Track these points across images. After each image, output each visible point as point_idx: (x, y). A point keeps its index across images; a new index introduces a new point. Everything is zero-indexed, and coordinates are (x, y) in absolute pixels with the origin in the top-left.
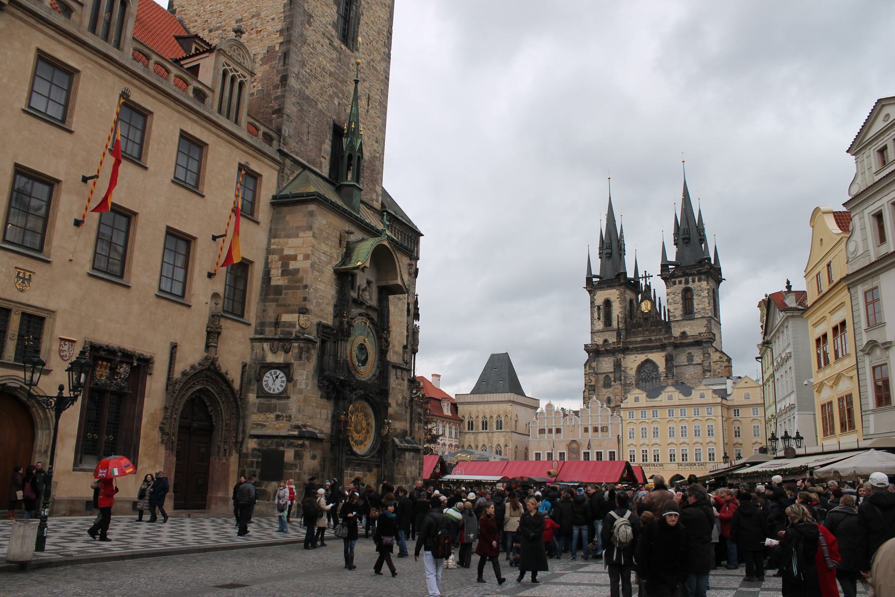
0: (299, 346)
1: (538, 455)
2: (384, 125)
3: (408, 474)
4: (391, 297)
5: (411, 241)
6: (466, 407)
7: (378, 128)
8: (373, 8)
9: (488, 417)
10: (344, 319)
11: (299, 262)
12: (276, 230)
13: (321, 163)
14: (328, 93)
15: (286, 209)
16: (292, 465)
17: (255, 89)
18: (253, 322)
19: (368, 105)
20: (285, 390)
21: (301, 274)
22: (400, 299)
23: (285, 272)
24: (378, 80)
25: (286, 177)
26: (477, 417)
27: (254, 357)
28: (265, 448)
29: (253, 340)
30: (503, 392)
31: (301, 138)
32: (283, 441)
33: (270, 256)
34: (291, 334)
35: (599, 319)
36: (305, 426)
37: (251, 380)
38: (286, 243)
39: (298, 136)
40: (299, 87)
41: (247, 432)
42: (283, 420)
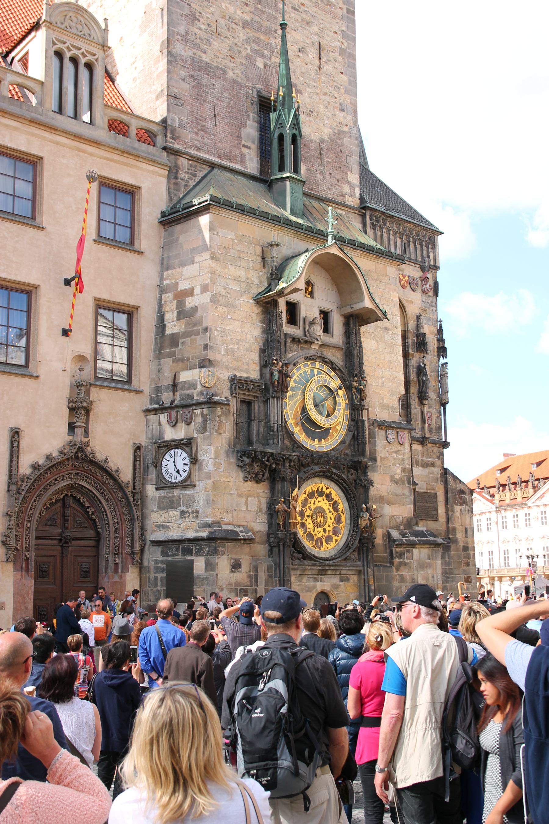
0: (202, 413)
2: (353, 83)
5: (421, 246)
7: (342, 90)
10: (274, 368)
11: (197, 297)
12: (169, 258)
13: (243, 155)
14: (244, 53)
16: (203, 579)
18: (147, 388)
19: (320, 59)
22: (386, 329)
23: (182, 314)
24: (334, 18)
25: (182, 183)
27: (150, 436)
28: (170, 558)
29: (148, 411)
31: (203, 126)
33: (163, 296)
34: (191, 397)
36: (218, 524)
37: (148, 467)
38: (181, 274)
39: (198, 123)
40: (190, 53)
41: (148, 537)
42: (189, 517)
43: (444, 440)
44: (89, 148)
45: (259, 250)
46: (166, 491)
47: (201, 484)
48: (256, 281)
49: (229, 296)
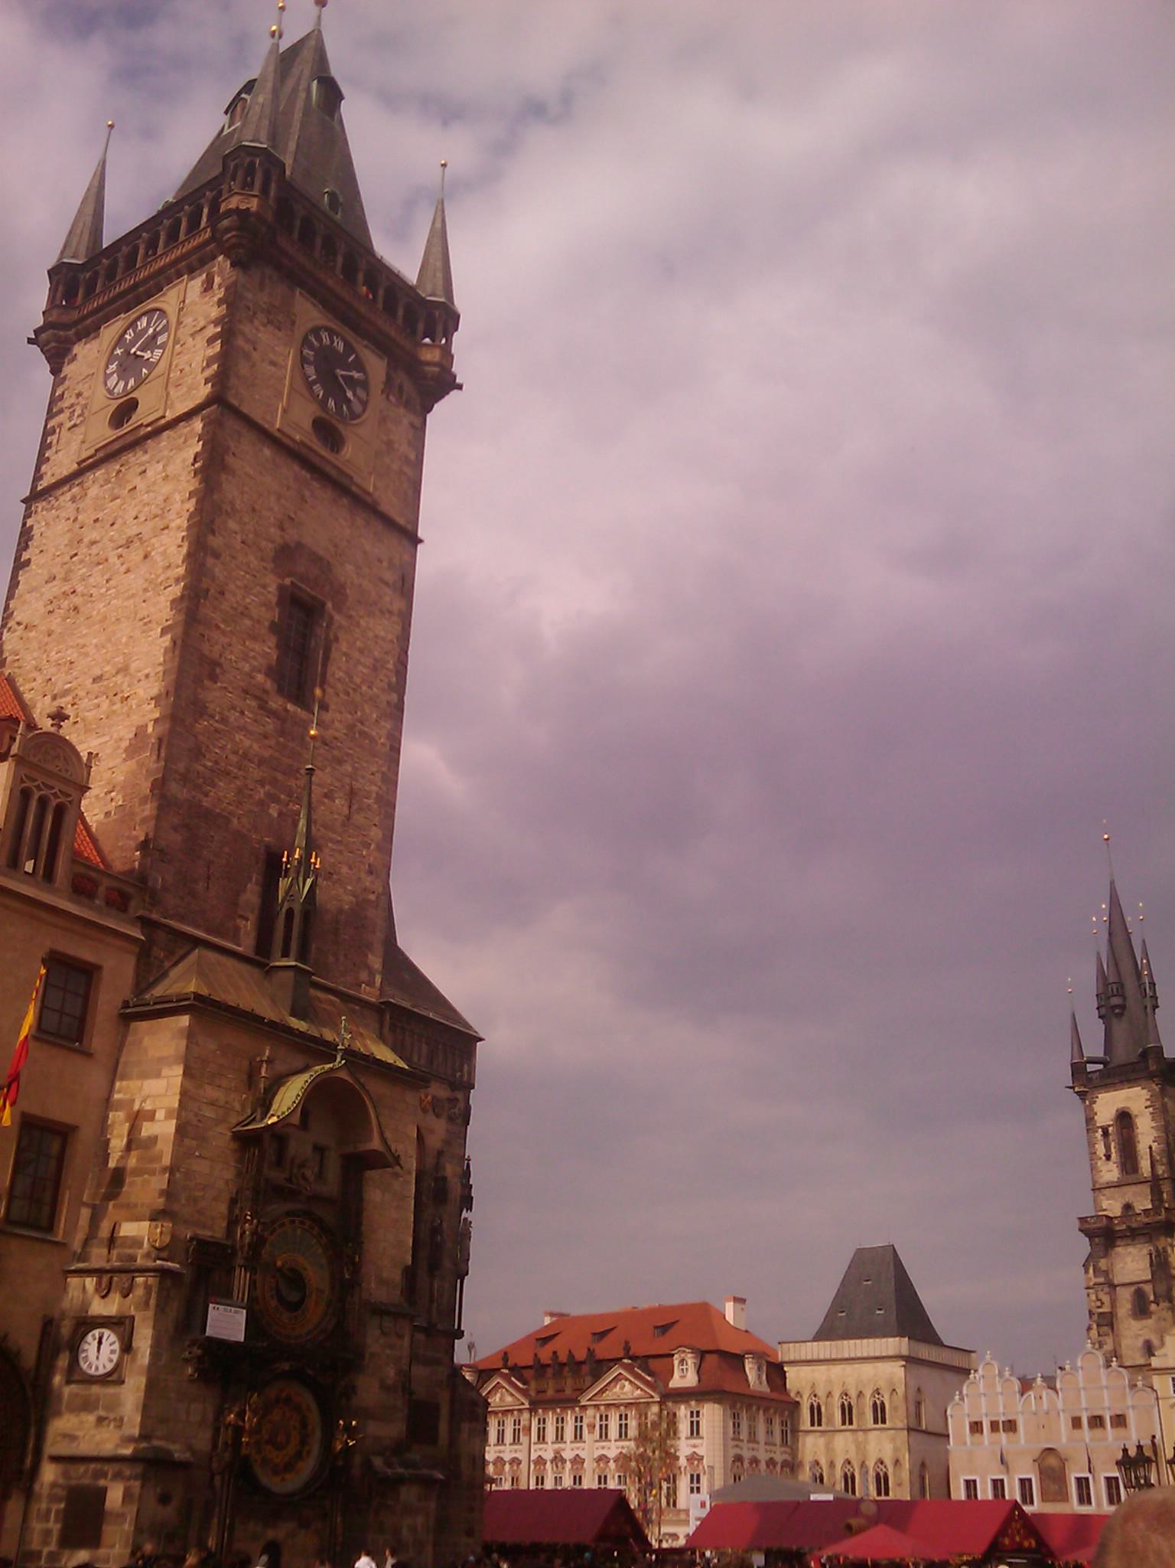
1: (971, 1485)
3: (405, 1531)
4: (369, 1174)
6: (805, 1371)
7: (373, 847)
8: (362, 622)
9: (853, 1393)
15: (144, 1025)
17: (113, 804)
19: (350, 807)
20: (118, 1367)
21: (159, 1146)
26: (829, 1394)
28: (74, 1482)
30: (885, 1336)
32: (106, 1468)
34: (133, 1259)
35: (1108, 1157)
42: (108, 1426)
43: (456, 1327)
44: (44, 915)
45: (246, 1063)
46: (80, 1386)
47: (132, 1381)
48: (237, 1106)
49: (201, 1125)
